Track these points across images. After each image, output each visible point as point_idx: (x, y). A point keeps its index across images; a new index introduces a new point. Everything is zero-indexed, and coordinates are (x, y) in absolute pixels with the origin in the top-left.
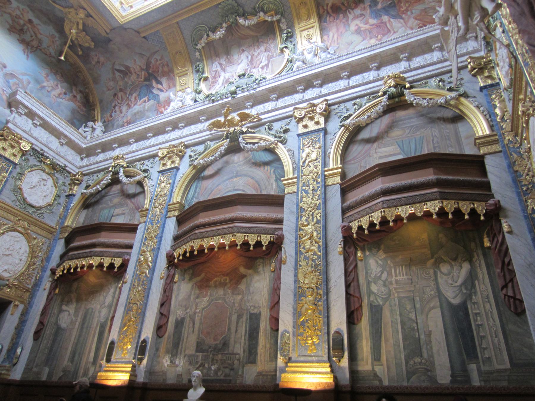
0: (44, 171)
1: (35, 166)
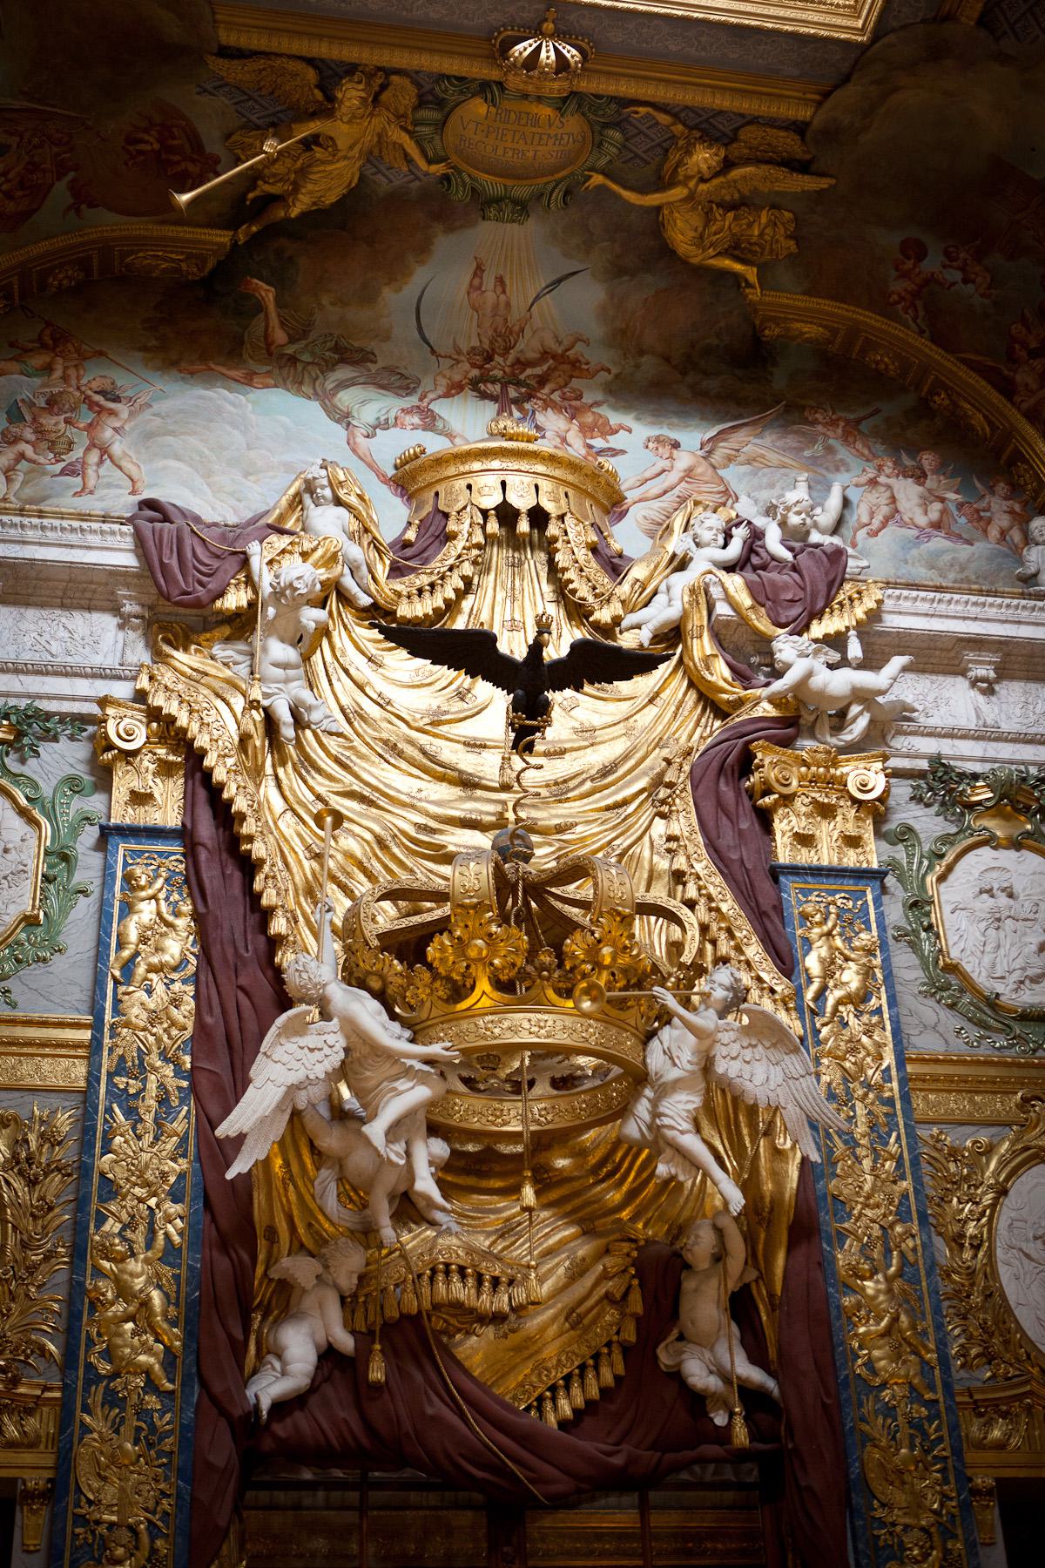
0: (990, 841)
1: (947, 839)
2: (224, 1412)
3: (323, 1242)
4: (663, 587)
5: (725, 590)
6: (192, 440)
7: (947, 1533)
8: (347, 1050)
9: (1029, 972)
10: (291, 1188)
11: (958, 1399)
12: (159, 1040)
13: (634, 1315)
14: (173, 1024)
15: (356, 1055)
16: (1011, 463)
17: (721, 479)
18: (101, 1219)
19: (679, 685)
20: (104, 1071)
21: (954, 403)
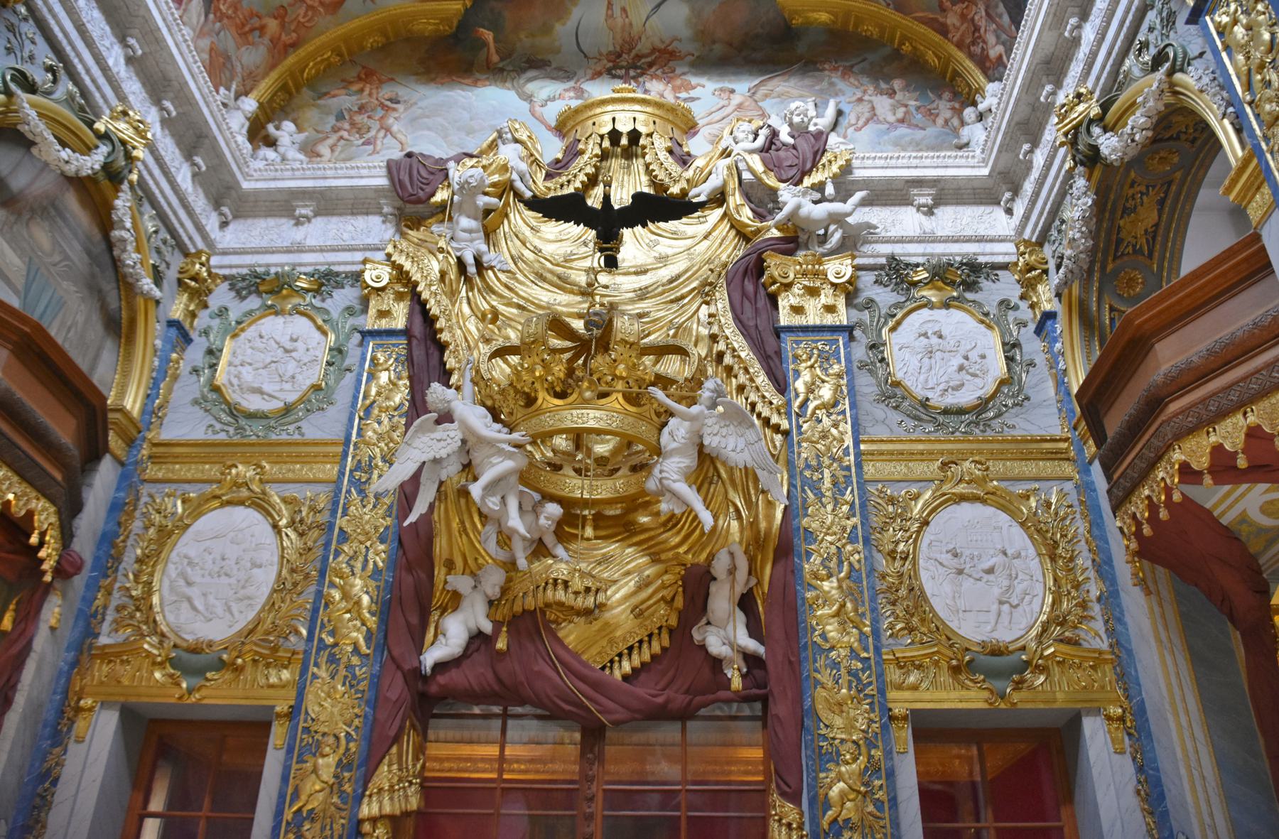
0: (929, 305)
1: (898, 305)
2: (399, 667)
4: (714, 170)
5: (747, 163)
6: (440, 120)
7: (871, 745)
8: (464, 442)
10: (464, 536)
11: (885, 657)
12: (382, 450)
13: (676, 609)
14: (392, 440)
15: (469, 444)
16: (952, 79)
17: (761, 108)
18: (337, 554)
19: (725, 226)
20: (348, 469)
21: (915, 48)
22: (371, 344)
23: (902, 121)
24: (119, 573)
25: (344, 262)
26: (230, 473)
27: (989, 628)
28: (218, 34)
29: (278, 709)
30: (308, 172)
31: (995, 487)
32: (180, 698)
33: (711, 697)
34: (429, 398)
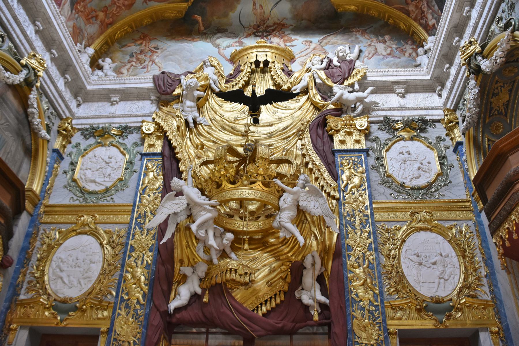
0: (404, 139)
1: (389, 139)
2: (158, 310)
3: (196, 263)
6: (177, 56)
8: (188, 205)
9: (415, 176)
10: (188, 249)
11: (385, 304)
12: (150, 208)
14: (155, 204)
15: (191, 206)
16: (412, 35)
17: (324, 49)
18: (130, 257)
19: (309, 104)
20: (135, 217)
21: (395, 21)
22: (145, 160)
23: (389, 54)
24: (30, 266)
25: (133, 122)
26: (80, 220)
27: (434, 290)
28: (77, 19)
29: (102, 329)
30: (117, 81)
31: (436, 224)
32: (57, 324)
33: (304, 324)
34: (172, 185)
